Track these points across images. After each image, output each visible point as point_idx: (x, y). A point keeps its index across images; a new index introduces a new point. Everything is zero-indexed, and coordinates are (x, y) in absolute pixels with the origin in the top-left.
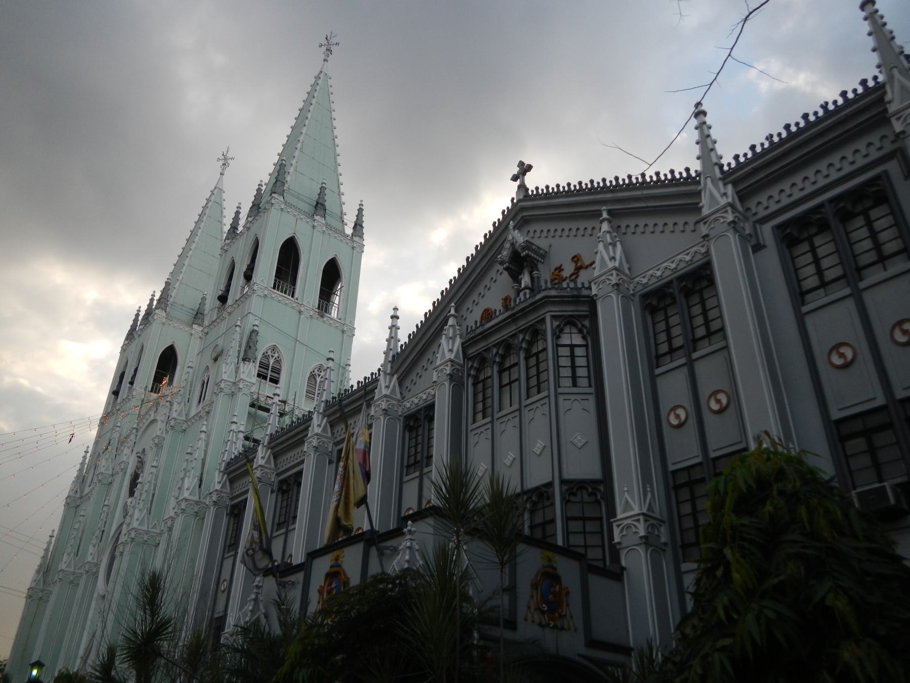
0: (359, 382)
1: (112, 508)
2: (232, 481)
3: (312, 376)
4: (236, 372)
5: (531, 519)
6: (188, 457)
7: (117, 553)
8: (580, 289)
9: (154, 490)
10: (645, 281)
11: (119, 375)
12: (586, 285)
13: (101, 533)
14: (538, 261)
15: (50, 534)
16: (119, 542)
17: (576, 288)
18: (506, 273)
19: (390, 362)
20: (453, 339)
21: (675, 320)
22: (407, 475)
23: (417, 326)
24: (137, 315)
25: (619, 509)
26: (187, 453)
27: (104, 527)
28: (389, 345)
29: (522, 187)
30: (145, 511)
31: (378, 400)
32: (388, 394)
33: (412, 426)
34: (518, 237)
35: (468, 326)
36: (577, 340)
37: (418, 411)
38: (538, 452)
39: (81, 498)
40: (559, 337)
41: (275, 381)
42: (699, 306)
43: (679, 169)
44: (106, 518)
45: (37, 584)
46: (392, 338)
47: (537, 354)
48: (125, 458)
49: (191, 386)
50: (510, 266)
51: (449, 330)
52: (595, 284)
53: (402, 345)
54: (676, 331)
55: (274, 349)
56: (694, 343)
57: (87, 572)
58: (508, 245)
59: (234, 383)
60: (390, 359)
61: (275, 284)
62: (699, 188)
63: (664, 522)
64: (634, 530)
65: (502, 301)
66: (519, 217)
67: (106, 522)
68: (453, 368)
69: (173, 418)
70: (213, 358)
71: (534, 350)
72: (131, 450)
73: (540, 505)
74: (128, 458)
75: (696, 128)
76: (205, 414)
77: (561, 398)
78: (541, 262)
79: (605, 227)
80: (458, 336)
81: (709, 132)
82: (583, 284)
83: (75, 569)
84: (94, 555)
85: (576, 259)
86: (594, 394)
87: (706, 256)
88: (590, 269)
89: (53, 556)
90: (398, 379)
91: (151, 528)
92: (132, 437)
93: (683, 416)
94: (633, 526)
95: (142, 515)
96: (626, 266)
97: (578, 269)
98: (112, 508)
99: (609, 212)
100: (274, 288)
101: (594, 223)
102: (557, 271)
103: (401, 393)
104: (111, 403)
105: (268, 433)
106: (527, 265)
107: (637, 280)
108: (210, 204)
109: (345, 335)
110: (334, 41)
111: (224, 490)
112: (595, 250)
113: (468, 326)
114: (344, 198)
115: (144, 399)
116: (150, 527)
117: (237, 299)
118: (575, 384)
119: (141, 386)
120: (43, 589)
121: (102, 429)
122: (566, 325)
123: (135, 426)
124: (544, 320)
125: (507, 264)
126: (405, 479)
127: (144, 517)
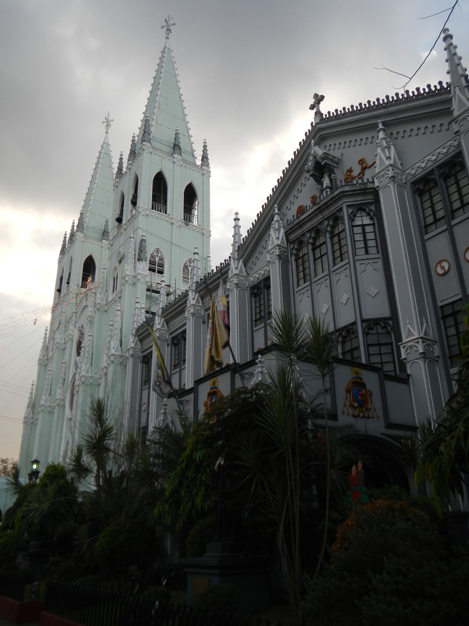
0: (217, 267)
1: (67, 364)
2: (141, 341)
3: (186, 267)
4: (135, 269)
5: (343, 348)
6: (111, 327)
7: (75, 392)
8: (366, 183)
9: (92, 350)
10: (413, 172)
11: (59, 278)
12: (371, 180)
14: (334, 167)
15: (32, 383)
16: (75, 385)
17: (364, 184)
18: (311, 178)
19: (236, 251)
20: (278, 230)
21: (437, 198)
22: (255, 327)
23: (253, 224)
24: (65, 238)
25: (404, 336)
26: (110, 325)
27: (65, 376)
28: (234, 239)
29: (318, 113)
30: (89, 364)
31: (231, 278)
32: (237, 273)
33: (256, 293)
34: (318, 151)
35: (288, 220)
36: (367, 221)
37: (259, 283)
38: (344, 302)
39: (47, 359)
40: (353, 220)
41: (161, 272)
42: (455, 186)
43: (434, 83)
44: (65, 370)
45: (28, 415)
46: (236, 234)
47: (338, 234)
48: (71, 332)
49: (106, 282)
50: (314, 173)
51: (275, 224)
52: (377, 178)
53: (243, 239)
54: (439, 206)
55: (158, 250)
56: (452, 213)
57: (58, 405)
58: (311, 158)
59: (134, 276)
60: (237, 249)
61: (153, 206)
62: (450, 96)
63: (436, 342)
64: (415, 349)
65: (310, 199)
66: (318, 136)
67: (65, 373)
68: (280, 250)
69: (98, 303)
70: (118, 261)
71: (336, 232)
72: (74, 326)
73: (348, 338)
74: (73, 332)
75: (445, 49)
76: (118, 298)
77: (358, 263)
78: (336, 167)
79: (381, 135)
80: (282, 228)
81: (455, 51)
82: (368, 180)
83: (50, 404)
84: (61, 395)
85: (361, 162)
86: (381, 258)
87: (458, 148)
88: (372, 168)
89: (36, 397)
90: (243, 262)
91: (94, 375)
93: (447, 267)
94: (414, 346)
95: (87, 367)
96: (399, 163)
97: (364, 169)
98: (67, 364)
99: (384, 123)
100: (152, 209)
101: (373, 133)
102: (349, 173)
103: (246, 272)
104: (57, 298)
105: (161, 307)
106: (326, 171)
107: (407, 172)
108: (102, 155)
109: (204, 236)
110: (171, 22)
111: (136, 347)
112: (375, 154)
113: (288, 220)
114: (192, 139)
116: (93, 374)
117: (129, 219)
118: (367, 253)
119: (74, 285)
120: (33, 417)
121: (53, 314)
122: (358, 210)
123: (75, 311)
124: (341, 209)
125: (312, 172)
126: (255, 329)
127: (88, 368)
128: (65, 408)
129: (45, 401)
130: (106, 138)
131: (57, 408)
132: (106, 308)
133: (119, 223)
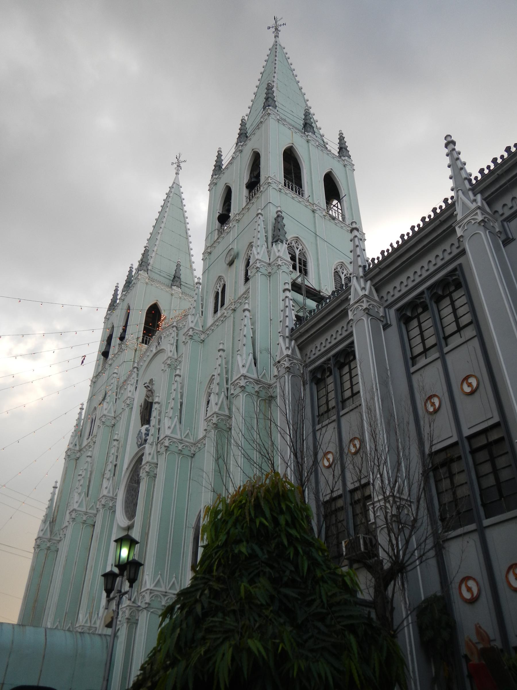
1: (122, 442)
6: (221, 353)
7: (143, 474)
13: (114, 467)
15: (54, 485)
16: (143, 463)
24: (116, 290)
27: (116, 461)
30: (176, 419)
39: (80, 450)
44: (117, 452)
48: (130, 395)
49: (202, 300)
57: (104, 506)
59: (269, 264)
67: (117, 457)
69: (191, 328)
70: (227, 262)
72: (134, 387)
74: (133, 394)
83: (87, 509)
89: (58, 506)
92: (134, 375)
98: (122, 442)
115: (136, 349)
117: (243, 207)
120: (50, 539)
128: (114, 512)
129: (78, 504)
130: (176, 178)
131: (102, 511)
132: (203, 337)
133: (220, 224)
